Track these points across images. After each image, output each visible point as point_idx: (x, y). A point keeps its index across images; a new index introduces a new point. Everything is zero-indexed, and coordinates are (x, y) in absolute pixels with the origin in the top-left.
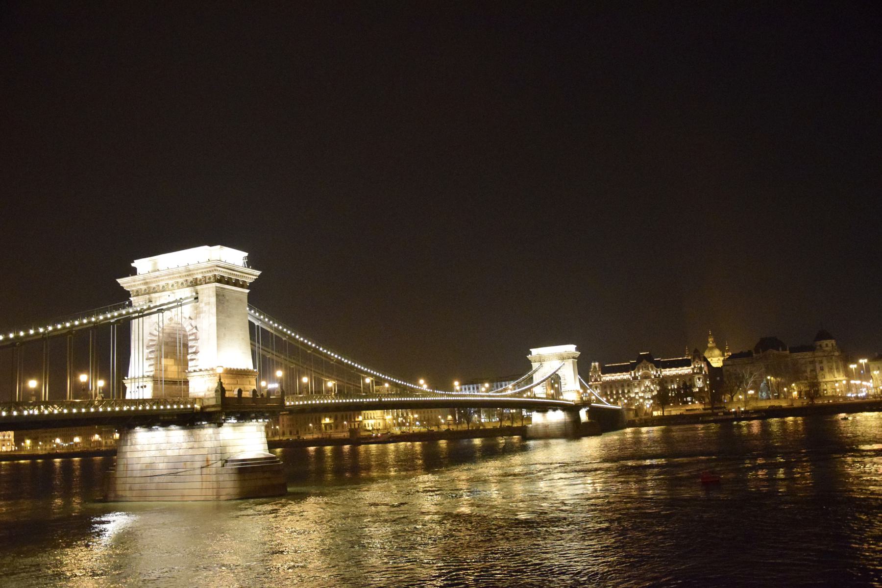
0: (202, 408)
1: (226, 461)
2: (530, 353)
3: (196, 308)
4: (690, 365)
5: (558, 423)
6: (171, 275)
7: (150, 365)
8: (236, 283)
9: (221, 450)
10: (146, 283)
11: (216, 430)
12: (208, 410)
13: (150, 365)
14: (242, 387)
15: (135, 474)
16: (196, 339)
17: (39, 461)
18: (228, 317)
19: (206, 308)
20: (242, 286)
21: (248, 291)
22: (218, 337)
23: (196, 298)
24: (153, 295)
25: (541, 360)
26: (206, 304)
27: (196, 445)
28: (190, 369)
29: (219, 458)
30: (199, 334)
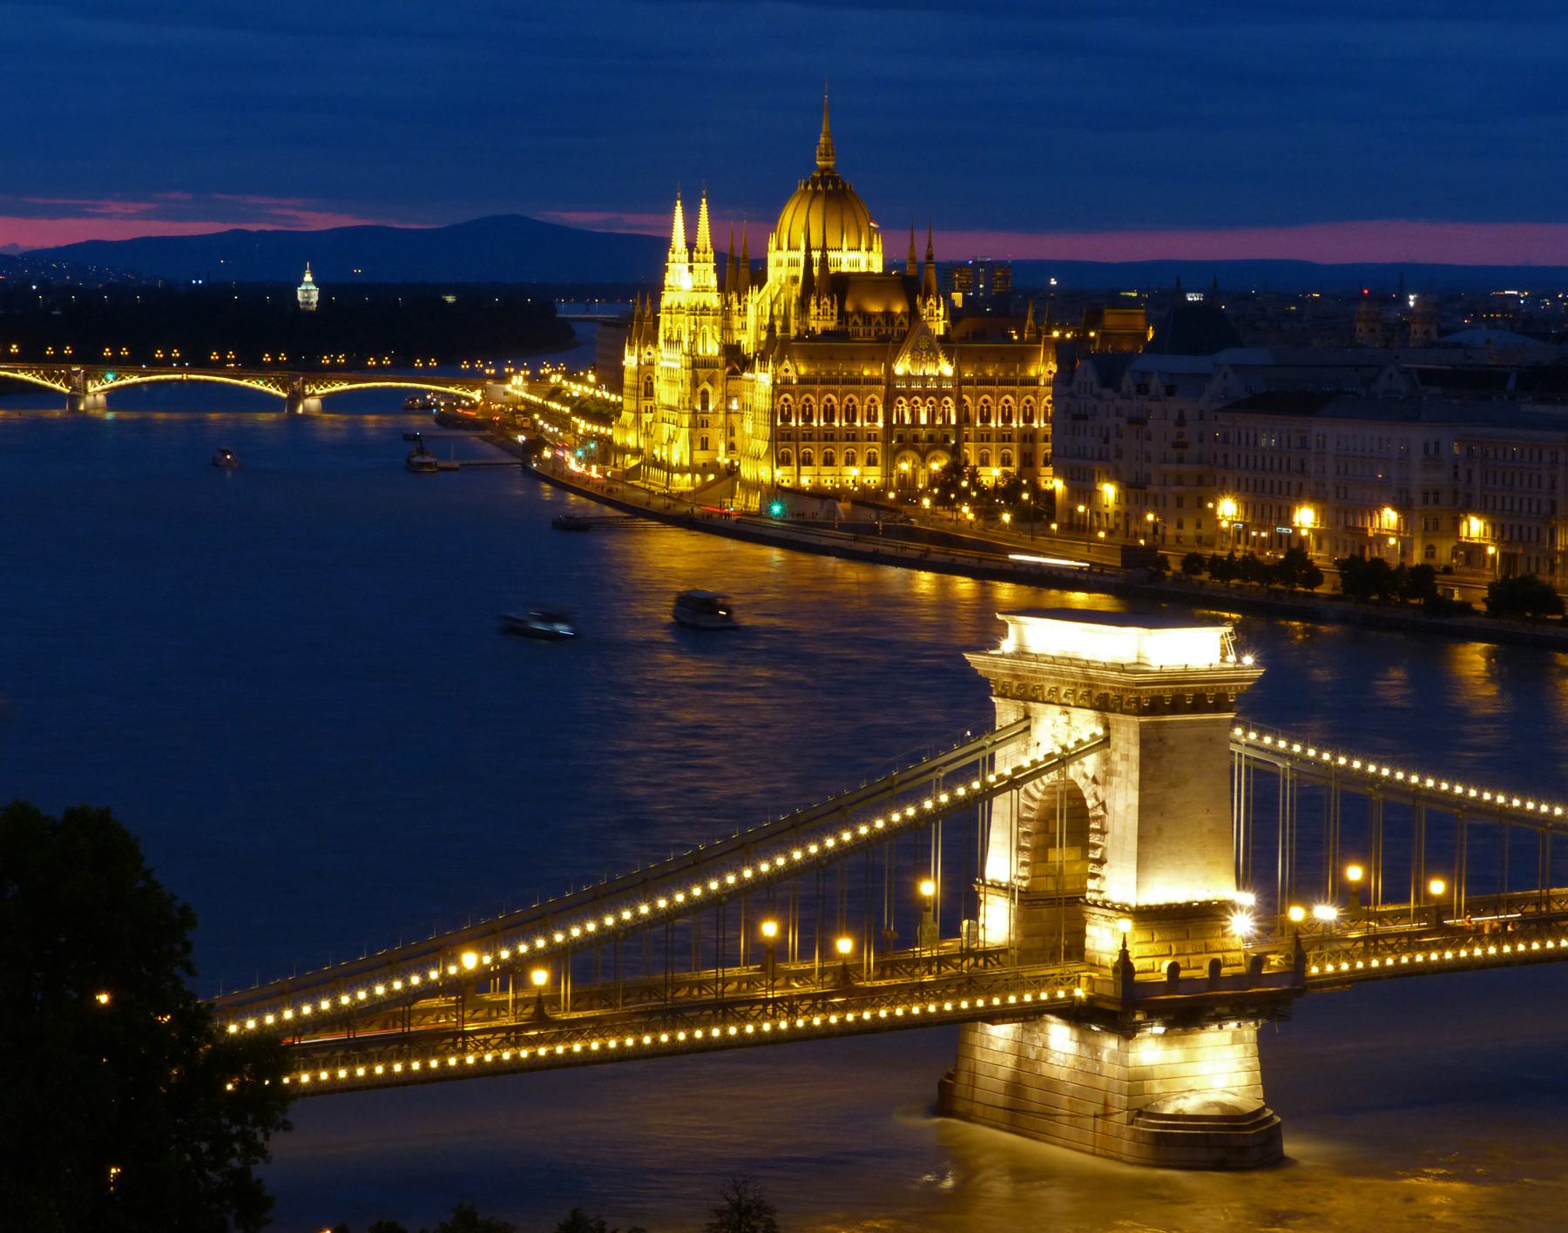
0: (1089, 998)
1: (1140, 1113)
3: (1106, 760)
7: (1024, 864)
8: (1199, 705)
9: (1137, 1081)
11: (1123, 1044)
12: (1101, 1004)
13: (1024, 864)
14: (1181, 960)
16: (1103, 832)
18: (1173, 785)
19: (1121, 767)
20: (1219, 707)
22: (1140, 838)
23: (1106, 741)
24: (1031, 704)
29: (1125, 1105)
30: (1109, 820)
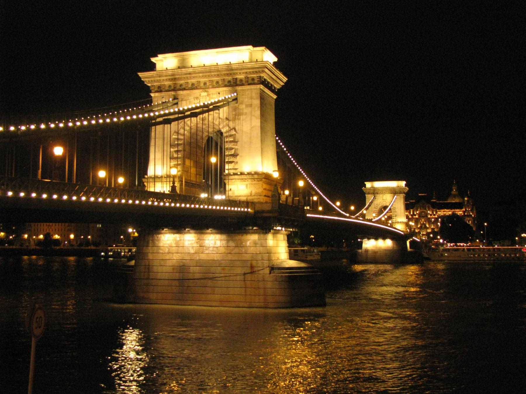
2: (365, 186)
3: (235, 109)
4: (462, 208)
5: (386, 250)
6: (207, 71)
10: (172, 80)
11: (262, 235)
15: (160, 276)
17: (72, 258)
21: (275, 97)
22: (261, 141)
25: (375, 192)
26: (247, 106)
27: (236, 250)
28: (227, 172)
30: (237, 136)
